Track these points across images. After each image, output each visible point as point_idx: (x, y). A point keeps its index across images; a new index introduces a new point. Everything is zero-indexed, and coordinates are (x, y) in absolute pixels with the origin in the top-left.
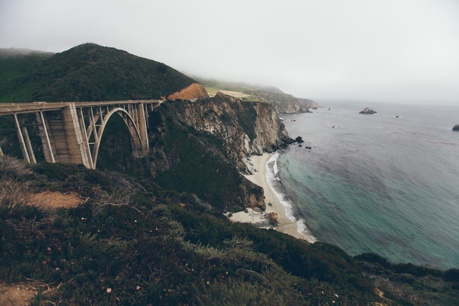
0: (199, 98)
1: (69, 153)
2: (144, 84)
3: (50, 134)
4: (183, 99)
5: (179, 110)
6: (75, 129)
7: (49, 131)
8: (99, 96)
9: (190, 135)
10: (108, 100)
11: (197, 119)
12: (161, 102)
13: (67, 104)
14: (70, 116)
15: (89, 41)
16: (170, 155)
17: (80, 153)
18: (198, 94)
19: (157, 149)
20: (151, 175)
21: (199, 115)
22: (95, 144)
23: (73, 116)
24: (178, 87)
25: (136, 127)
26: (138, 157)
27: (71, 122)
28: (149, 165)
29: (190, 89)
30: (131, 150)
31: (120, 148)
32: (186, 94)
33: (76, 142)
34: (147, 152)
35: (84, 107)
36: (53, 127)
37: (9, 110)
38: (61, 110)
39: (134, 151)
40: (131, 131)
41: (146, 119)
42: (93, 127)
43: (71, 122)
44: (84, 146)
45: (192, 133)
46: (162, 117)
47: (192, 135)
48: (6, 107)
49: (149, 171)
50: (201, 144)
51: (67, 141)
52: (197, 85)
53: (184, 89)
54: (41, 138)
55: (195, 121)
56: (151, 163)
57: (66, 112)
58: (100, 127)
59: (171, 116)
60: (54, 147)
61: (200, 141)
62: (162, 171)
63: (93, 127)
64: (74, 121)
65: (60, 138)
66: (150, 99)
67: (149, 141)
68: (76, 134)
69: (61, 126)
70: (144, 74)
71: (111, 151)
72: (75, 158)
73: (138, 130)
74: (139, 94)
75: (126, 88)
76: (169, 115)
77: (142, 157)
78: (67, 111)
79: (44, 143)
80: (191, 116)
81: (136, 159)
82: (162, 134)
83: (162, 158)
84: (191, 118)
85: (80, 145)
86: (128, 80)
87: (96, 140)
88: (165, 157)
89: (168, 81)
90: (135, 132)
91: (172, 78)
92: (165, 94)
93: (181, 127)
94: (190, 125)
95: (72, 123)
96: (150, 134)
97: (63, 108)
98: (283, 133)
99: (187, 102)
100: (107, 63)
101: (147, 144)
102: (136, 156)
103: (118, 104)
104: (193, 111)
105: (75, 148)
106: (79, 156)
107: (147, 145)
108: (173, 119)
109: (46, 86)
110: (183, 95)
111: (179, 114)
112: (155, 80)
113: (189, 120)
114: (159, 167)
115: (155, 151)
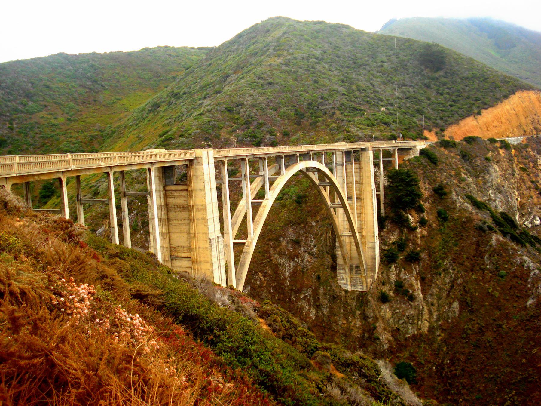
0: (535, 132)
1: (191, 258)
2: (382, 101)
3: (164, 214)
4: (484, 135)
5: (470, 168)
6: (208, 206)
7: (163, 208)
8: (278, 134)
9: (496, 238)
10: (295, 143)
11: (525, 192)
12: (421, 145)
13: (199, 152)
14: (201, 177)
15: (274, 15)
16: (435, 290)
17: (212, 260)
18: (533, 122)
19: (400, 271)
20: (377, 342)
21: (532, 182)
22: (246, 244)
23: (206, 178)
24: (473, 104)
25: (349, 211)
26: (349, 288)
27: (201, 190)
28: (374, 311)
29: (508, 107)
30: (334, 268)
31: (309, 262)
32: (496, 123)
33: (206, 234)
34: (373, 277)
35: (232, 158)
36: (171, 201)
37: (102, 164)
38: (187, 165)
39: (341, 271)
40: (336, 220)
41: (378, 189)
42: (247, 203)
43: (201, 190)
44: (220, 243)
45: (504, 234)
46: (421, 184)
47: (501, 239)
48: (98, 159)
49: (375, 328)
50: (528, 267)
51: (192, 231)
52: (532, 95)
53: (490, 109)
54: (150, 221)
55: (516, 201)
56: (381, 309)
57: (196, 169)
58: (263, 205)
59: (447, 184)
60: (168, 241)
61: (524, 257)
62: (406, 333)
63: (247, 203)
64: (207, 188)
66: (394, 138)
67: (381, 249)
68: (208, 218)
70: (385, 76)
71: (290, 267)
72: (201, 269)
73: (354, 218)
74: (368, 125)
75: (338, 114)
76: (442, 182)
77: (359, 288)
78: (198, 167)
80: (506, 184)
81: (343, 292)
82: (418, 230)
83: (412, 298)
84: (506, 192)
85: (212, 241)
86: (344, 94)
87: (250, 233)
88: (421, 295)
89: (447, 90)
90: (347, 223)
91: (459, 80)
92: (436, 125)
93: (472, 214)
94: (501, 210)
95: (203, 193)
96: (385, 230)
97: (191, 161)
99: (498, 145)
100: (303, 58)
101: (375, 255)
102: (347, 285)
103: (309, 152)
104: (513, 171)
105: (204, 248)
106: (208, 266)
107: (375, 259)
108: (451, 192)
109: (184, 118)
110: (487, 126)
111: (470, 180)
112: (411, 89)
113: (499, 195)
114: (401, 322)
115: (393, 278)
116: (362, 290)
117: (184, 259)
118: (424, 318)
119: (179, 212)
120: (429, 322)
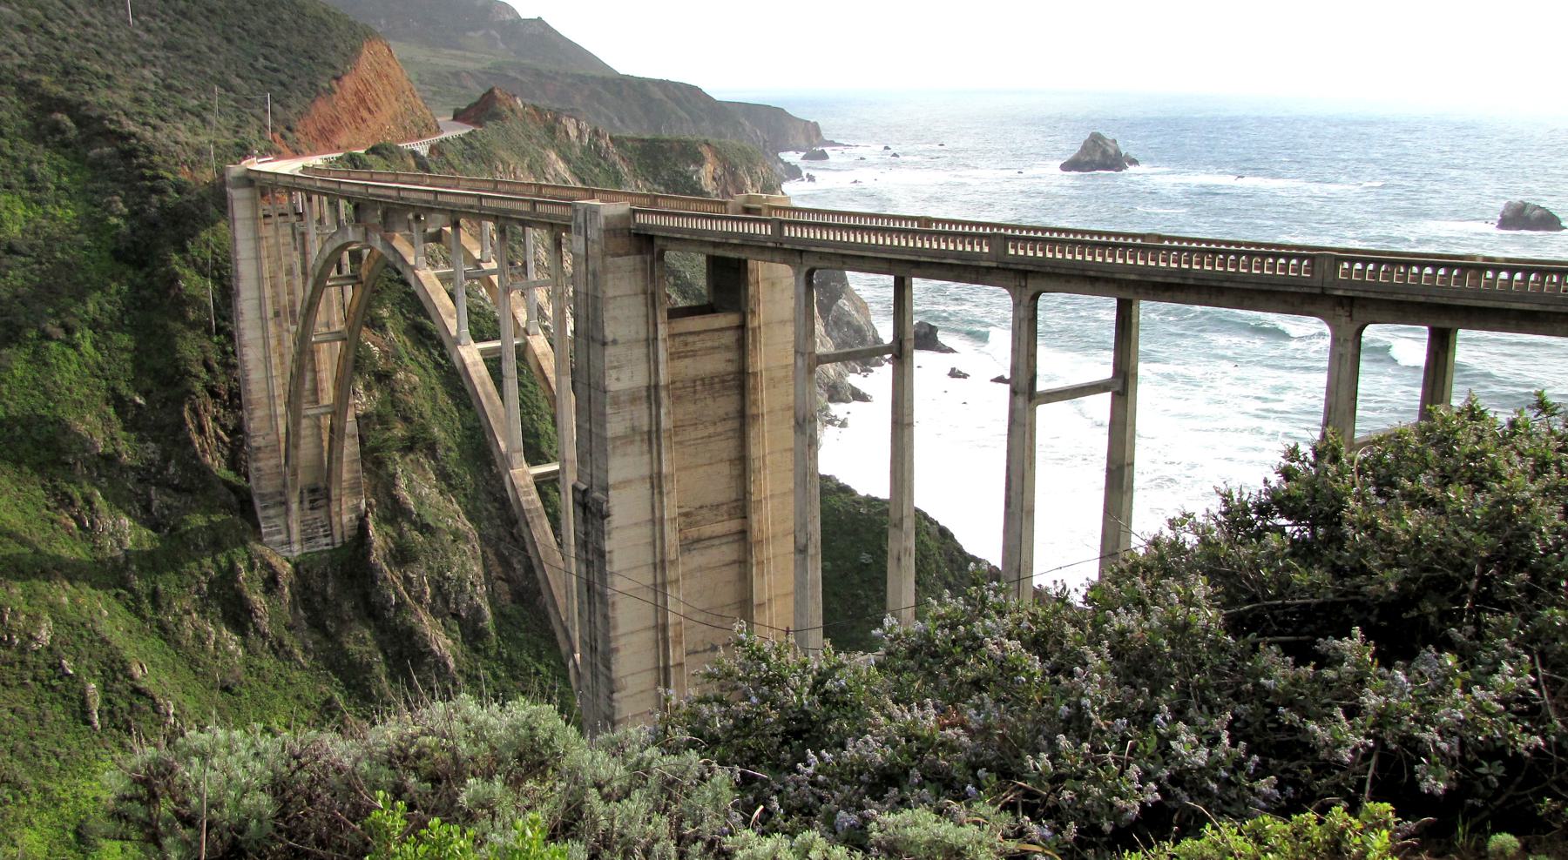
31: (169, 507)
51: (755, 451)
65: (710, 437)
69: (730, 355)
79: (627, 483)
98: (842, 313)
102: (289, 543)
116: (330, 547)
117: (716, 542)
118: (494, 574)
119: (709, 401)
120: (507, 581)
